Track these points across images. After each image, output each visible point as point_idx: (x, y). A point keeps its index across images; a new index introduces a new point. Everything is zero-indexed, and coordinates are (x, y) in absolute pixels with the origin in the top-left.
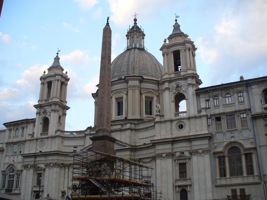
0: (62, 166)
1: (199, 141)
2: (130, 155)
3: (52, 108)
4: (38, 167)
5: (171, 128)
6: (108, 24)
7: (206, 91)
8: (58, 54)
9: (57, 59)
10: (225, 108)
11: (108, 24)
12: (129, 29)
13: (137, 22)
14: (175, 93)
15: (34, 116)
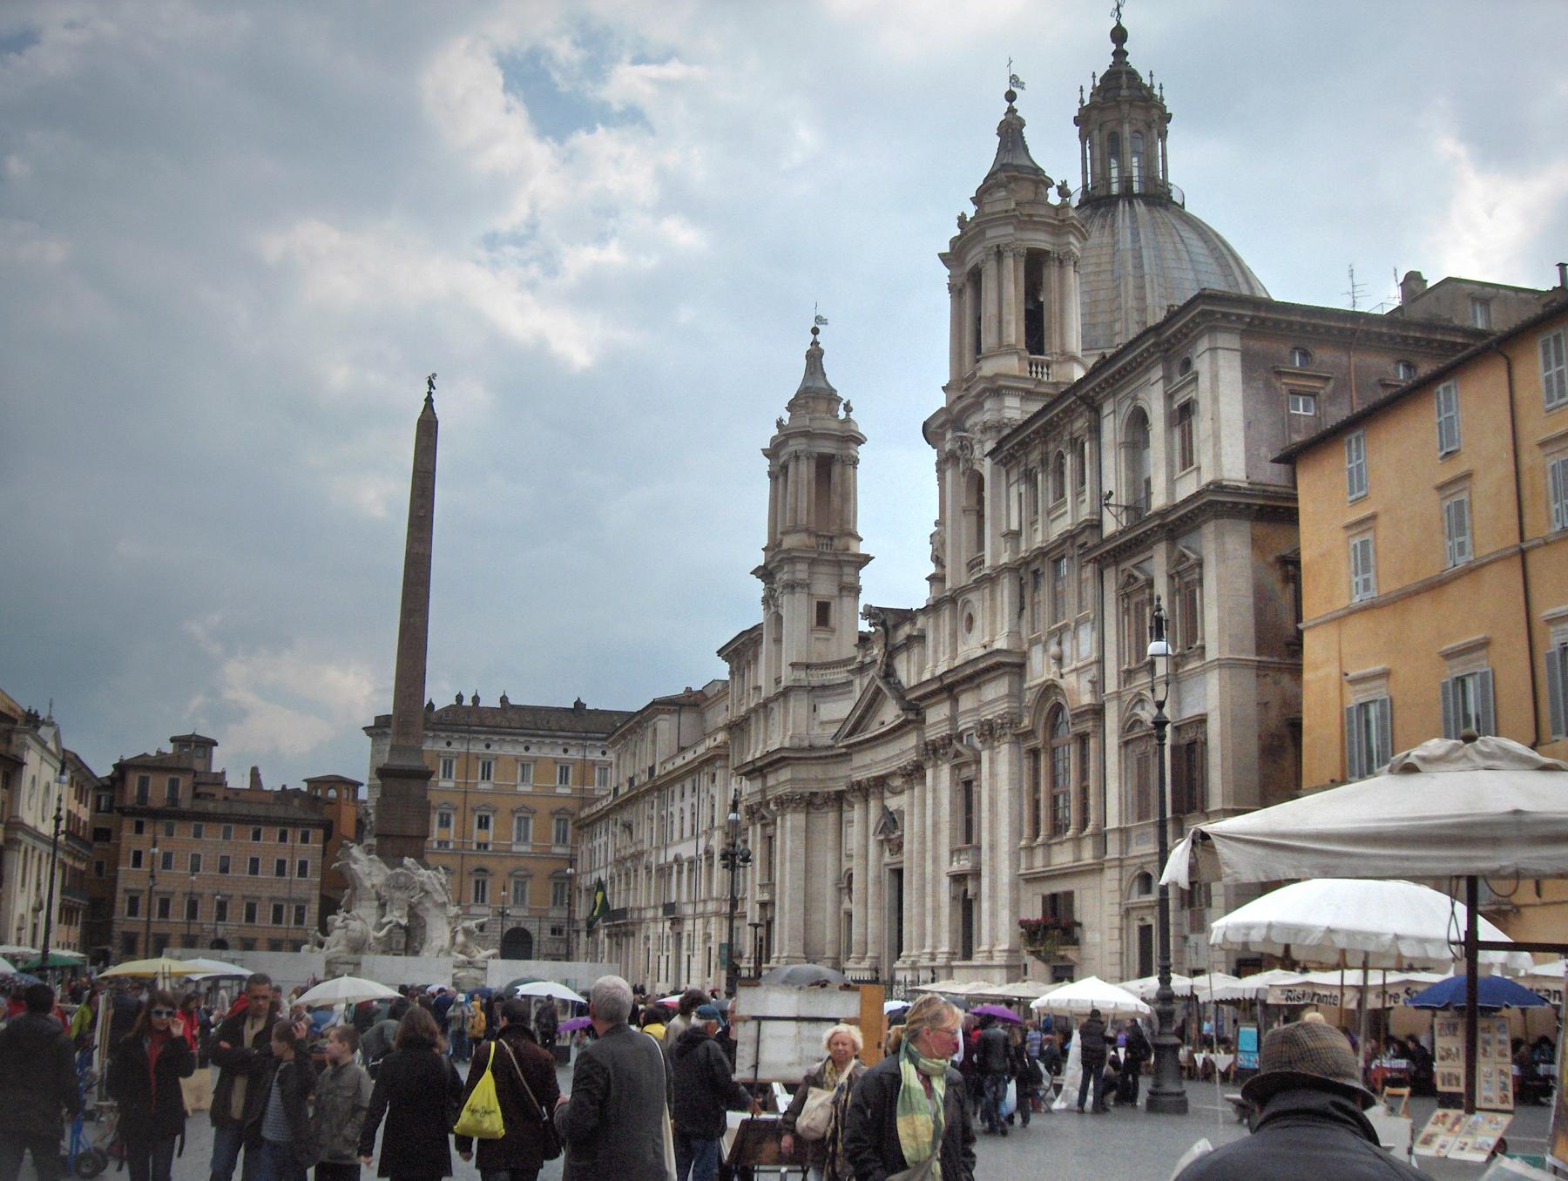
0: (818, 801)
1: (993, 684)
2: (916, 747)
3: (785, 577)
4: (763, 817)
5: (954, 635)
6: (429, 400)
7: (1012, 456)
8: (815, 331)
9: (815, 357)
10: (1054, 524)
11: (429, 400)
12: (1082, 101)
13: (1126, 46)
14: (964, 473)
15: (756, 615)
